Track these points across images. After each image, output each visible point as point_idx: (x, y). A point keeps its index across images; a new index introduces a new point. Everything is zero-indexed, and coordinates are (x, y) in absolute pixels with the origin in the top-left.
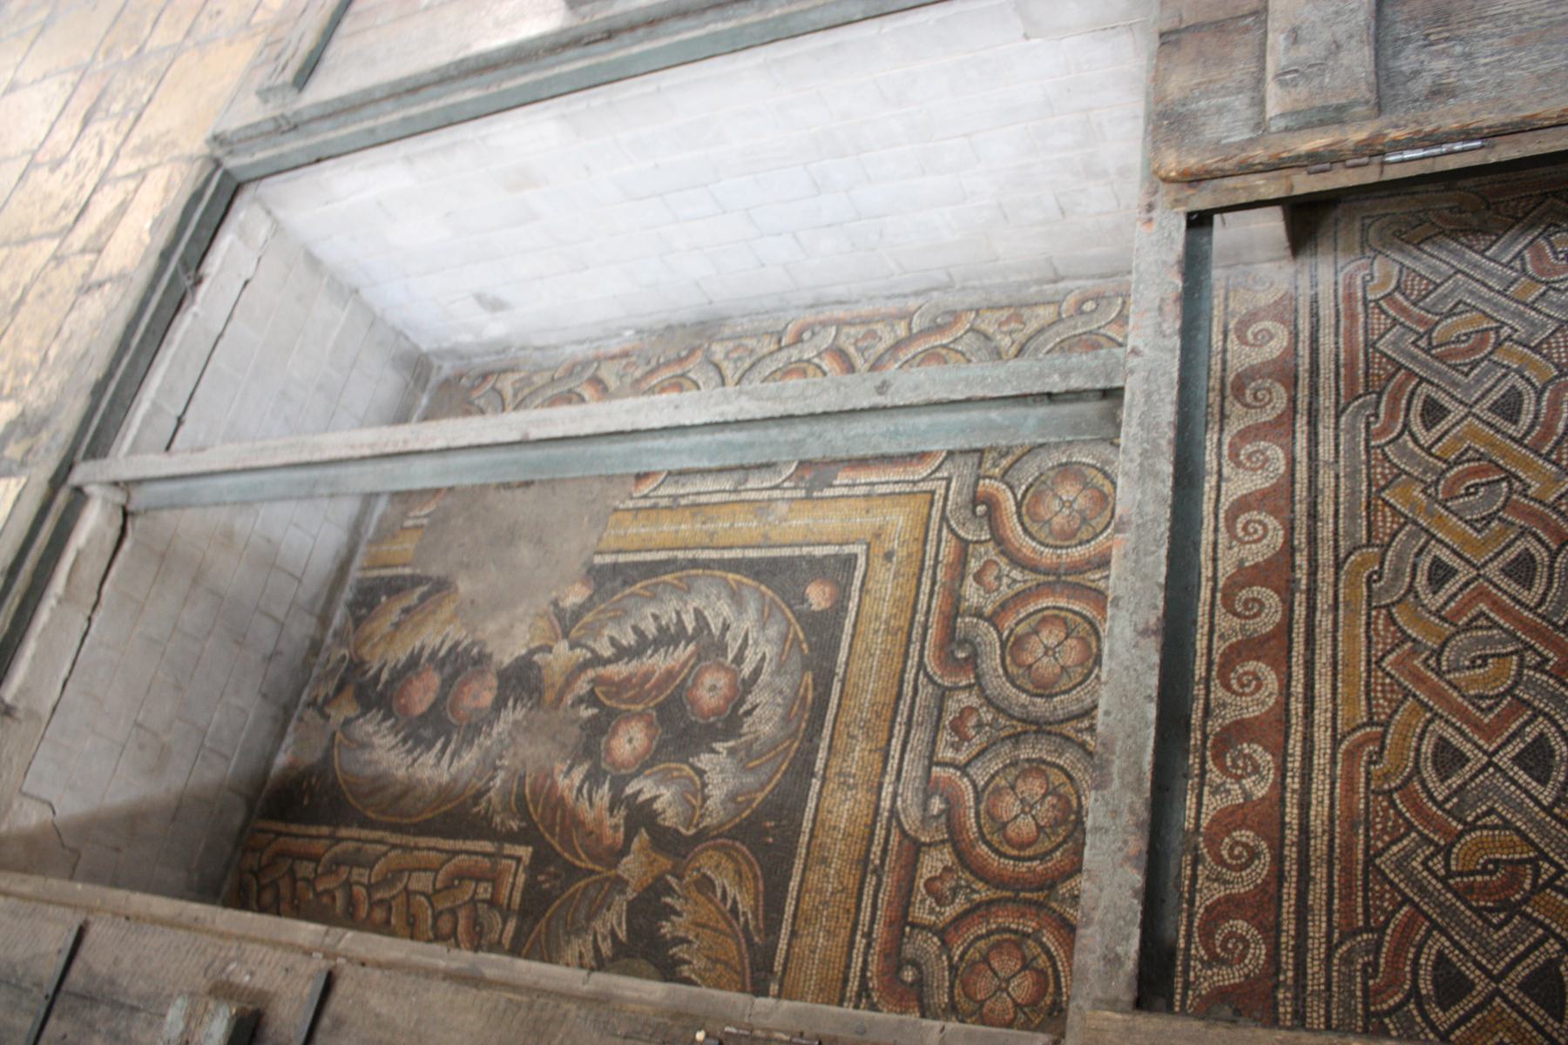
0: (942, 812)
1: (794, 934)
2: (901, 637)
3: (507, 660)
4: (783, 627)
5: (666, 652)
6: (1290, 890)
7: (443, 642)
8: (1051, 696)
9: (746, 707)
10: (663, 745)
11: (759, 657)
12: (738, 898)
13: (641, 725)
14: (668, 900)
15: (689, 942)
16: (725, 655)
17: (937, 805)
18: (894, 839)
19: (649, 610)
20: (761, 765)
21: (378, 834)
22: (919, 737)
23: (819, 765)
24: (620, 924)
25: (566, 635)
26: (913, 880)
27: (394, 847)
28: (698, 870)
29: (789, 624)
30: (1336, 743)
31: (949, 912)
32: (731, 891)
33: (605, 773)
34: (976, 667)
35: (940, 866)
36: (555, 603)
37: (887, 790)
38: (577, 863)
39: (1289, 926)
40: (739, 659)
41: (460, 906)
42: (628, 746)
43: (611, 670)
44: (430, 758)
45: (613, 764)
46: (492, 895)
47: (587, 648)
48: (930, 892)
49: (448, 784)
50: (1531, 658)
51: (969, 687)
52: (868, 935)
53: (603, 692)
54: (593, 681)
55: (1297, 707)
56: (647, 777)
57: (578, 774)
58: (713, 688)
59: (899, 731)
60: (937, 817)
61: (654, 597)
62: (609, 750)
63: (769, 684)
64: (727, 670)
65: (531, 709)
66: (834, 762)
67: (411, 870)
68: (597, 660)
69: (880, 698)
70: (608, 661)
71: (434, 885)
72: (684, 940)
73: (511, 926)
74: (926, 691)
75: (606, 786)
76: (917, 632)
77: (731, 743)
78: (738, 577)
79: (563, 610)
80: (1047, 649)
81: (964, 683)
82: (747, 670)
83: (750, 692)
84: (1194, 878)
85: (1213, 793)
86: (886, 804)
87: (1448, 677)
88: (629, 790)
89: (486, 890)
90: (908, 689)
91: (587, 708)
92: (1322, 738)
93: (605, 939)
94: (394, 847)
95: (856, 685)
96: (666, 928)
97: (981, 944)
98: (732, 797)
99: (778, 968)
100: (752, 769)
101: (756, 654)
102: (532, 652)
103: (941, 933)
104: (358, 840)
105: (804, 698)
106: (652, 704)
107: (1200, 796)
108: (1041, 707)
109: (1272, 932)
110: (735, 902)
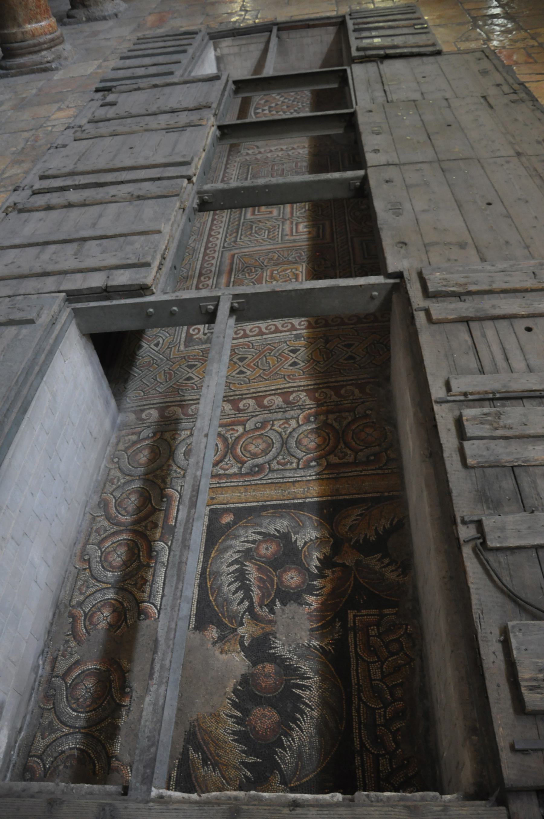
0: (315, 461)
1: (366, 493)
2: (248, 487)
3: (248, 663)
4: (240, 528)
5: (248, 574)
6: (331, 385)
7: (231, 716)
8: (273, 443)
9: (276, 533)
10: (293, 563)
11: (253, 534)
12: (356, 514)
13: (284, 575)
14: (361, 541)
15: (376, 528)
16: (251, 548)
17: (314, 463)
18: (326, 472)
19: (225, 589)
20: (301, 521)
21: (354, 713)
22: (288, 474)
23: (300, 501)
24: (375, 558)
25: (235, 630)
26: (340, 464)
27: (360, 699)
28: (347, 533)
29: (240, 526)
30: (290, 382)
31: (349, 452)
32: (353, 518)
33: (308, 585)
34: (262, 464)
35: (334, 458)
36: (214, 643)
37: (308, 478)
38: (352, 585)
39: (342, 383)
40: (254, 542)
41: (383, 642)
42: (295, 579)
43: (255, 599)
44: (304, 694)
45: (303, 583)
46: (374, 625)
47: (243, 615)
48: (344, 458)
49: (320, 675)
50: (268, 354)
51: (269, 465)
52: (361, 471)
53: (267, 601)
54: (261, 608)
55: (279, 391)
56: (308, 565)
57: (310, 599)
58: (267, 549)
59: (285, 480)
60: (317, 462)
61: (220, 588)
62: (297, 587)
63: (266, 528)
64: (258, 546)
65: (275, 638)
66: (299, 496)
67: (371, 680)
68: (251, 609)
69: (273, 488)
70: (252, 603)
71: (375, 662)
72: (376, 530)
73: (386, 611)
74: (270, 476)
75: (315, 583)
76: (246, 483)
77: (292, 534)
78: (214, 552)
79: (219, 637)
80: (256, 447)
81: (268, 466)
82: (260, 537)
83: (269, 533)
84: (330, 402)
85: (305, 402)
86: (314, 477)
87: (271, 366)
88: (316, 571)
89: (373, 630)
90: (270, 481)
91: (276, 606)
92: (288, 385)
93: (382, 563)
94: (360, 699)
95: (267, 497)
96: (373, 538)
97: (358, 442)
98: (315, 528)
99: (378, 495)
100: (303, 524)
101: (252, 536)
102: (243, 648)
103: (357, 453)
104: (360, 729)
105: (272, 513)
106: (274, 573)
107: (306, 405)
108: (277, 445)
109: (342, 386)
110: (357, 516)
